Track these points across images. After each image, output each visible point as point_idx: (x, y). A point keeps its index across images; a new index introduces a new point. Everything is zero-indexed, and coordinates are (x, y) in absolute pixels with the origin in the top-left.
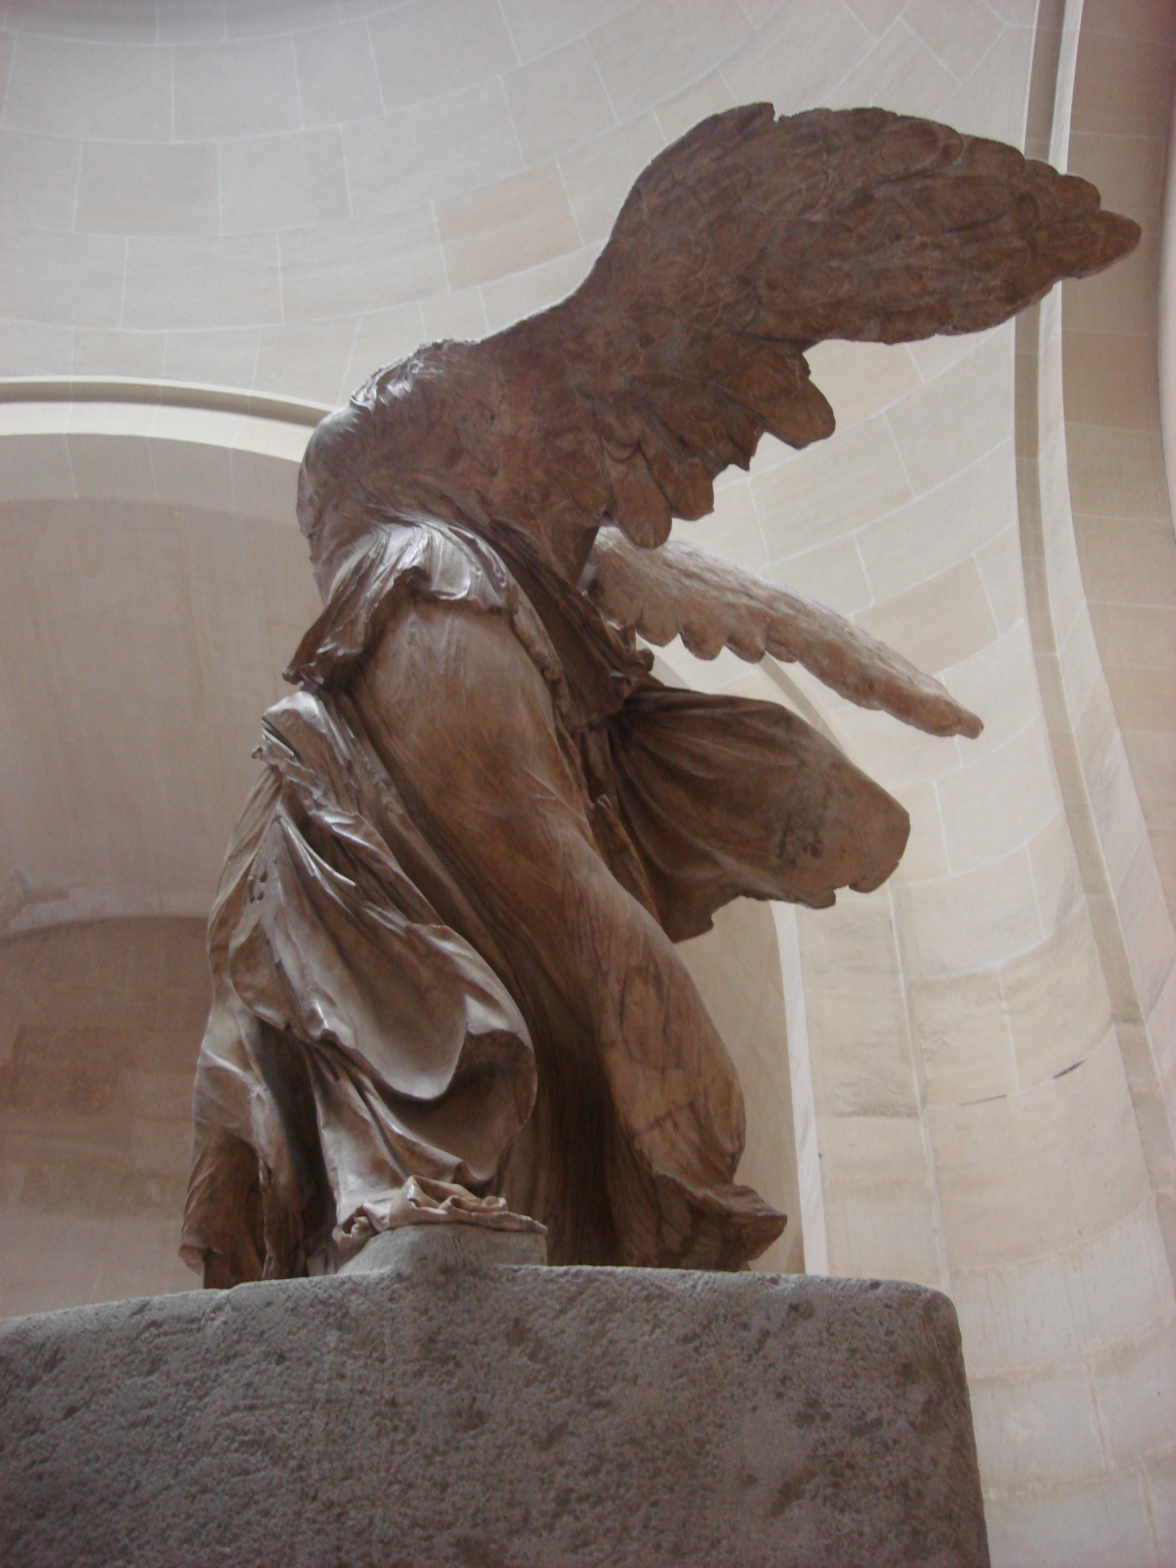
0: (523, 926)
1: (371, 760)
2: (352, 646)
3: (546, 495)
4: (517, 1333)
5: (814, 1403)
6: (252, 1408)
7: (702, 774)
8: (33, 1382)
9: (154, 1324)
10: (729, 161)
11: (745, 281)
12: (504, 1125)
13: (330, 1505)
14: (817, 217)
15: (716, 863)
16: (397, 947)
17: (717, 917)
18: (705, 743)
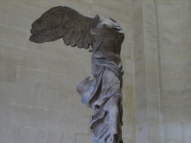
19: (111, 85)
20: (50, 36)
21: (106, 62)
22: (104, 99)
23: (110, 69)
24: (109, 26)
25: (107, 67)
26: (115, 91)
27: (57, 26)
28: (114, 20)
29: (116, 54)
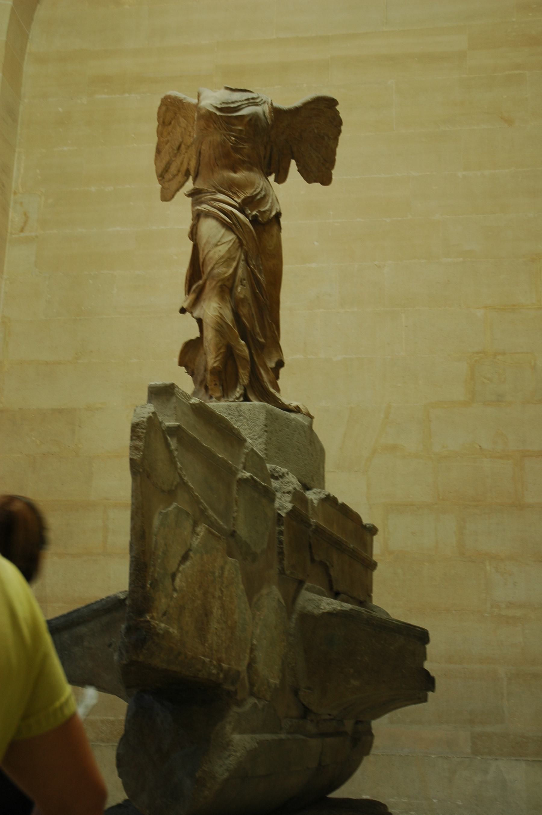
2: (263, 220)
14: (316, 131)
16: (266, 323)
19: (206, 252)
20: (177, 175)
21: (203, 199)
22: (194, 290)
23: (208, 215)
24: (205, 108)
25: (202, 211)
26: (212, 265)
27: (180, 147)
28: (233, 88)
29: (235, 172)
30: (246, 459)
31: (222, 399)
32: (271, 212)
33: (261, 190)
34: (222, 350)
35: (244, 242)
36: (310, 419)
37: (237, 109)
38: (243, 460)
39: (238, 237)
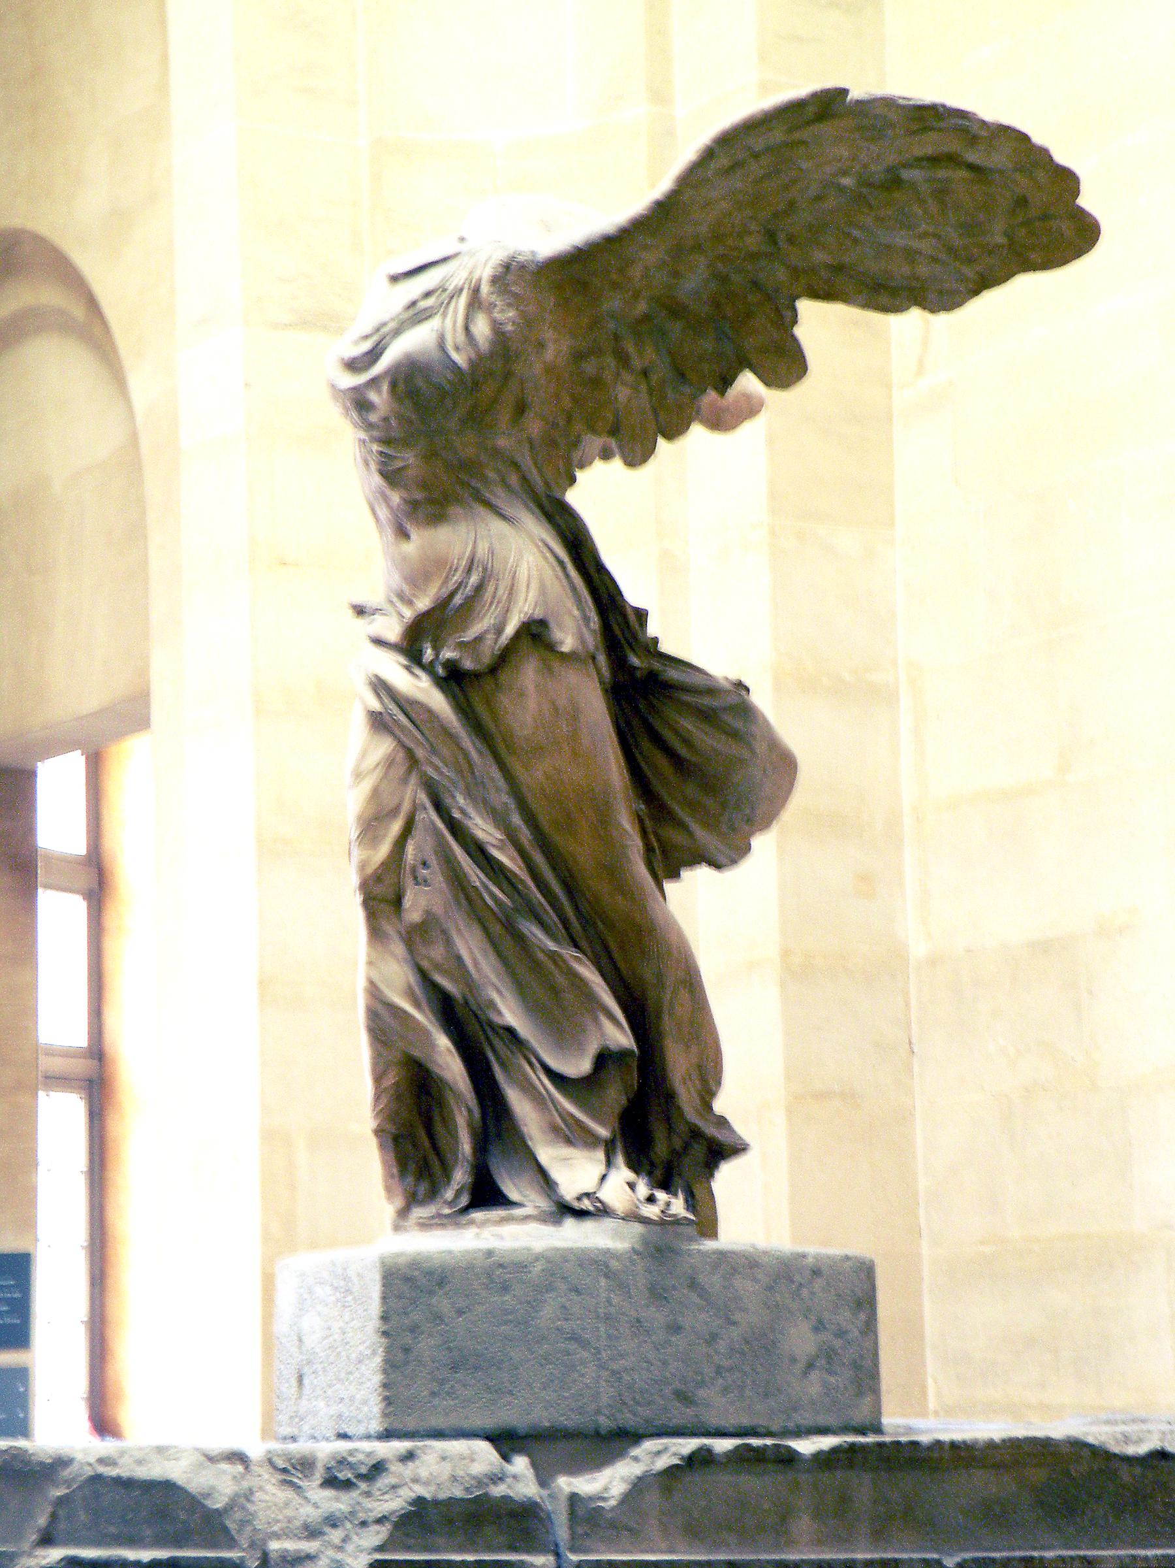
0: (599, 923)
1: (496, 773)
2: (477, 659)
3: (569, 420)
4: (693, 1284)
5: (820, 1322)
6: (566, 1320)
7: (683, 752)
8: (431, 1293)
9: (501, 1266)
10: (797, 135)
11: (771, 236)
12: (615, 1096)
13: (613, 1372)
14: (846, 181)
15: (690, 834)
17: (686, 874)
18: (688, 724)
30: (54, 1516)
31: (419, 1212)
32: (499, 630)
33: (469, 570)
34: (390, 1080)
35: (420, 753)
36: (638, 1228)
37: (374, 355)
38: (42, 1521)
39: (404, 746)
